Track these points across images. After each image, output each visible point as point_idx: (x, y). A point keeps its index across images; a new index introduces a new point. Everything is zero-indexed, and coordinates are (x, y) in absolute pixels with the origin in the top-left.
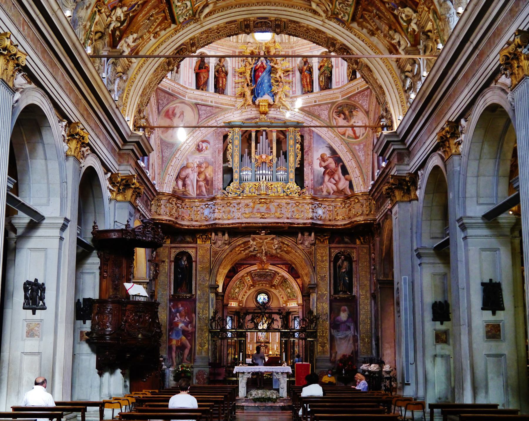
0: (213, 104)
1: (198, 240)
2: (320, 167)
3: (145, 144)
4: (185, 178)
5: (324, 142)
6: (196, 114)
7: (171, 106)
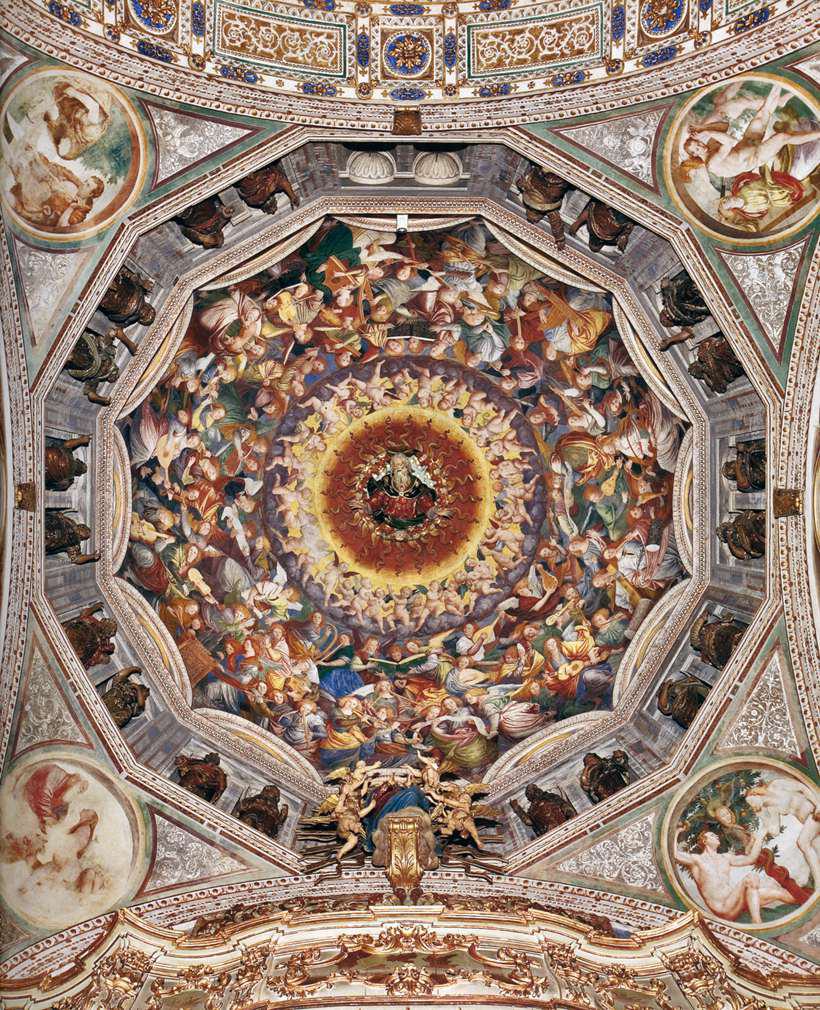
6: (141, 852)
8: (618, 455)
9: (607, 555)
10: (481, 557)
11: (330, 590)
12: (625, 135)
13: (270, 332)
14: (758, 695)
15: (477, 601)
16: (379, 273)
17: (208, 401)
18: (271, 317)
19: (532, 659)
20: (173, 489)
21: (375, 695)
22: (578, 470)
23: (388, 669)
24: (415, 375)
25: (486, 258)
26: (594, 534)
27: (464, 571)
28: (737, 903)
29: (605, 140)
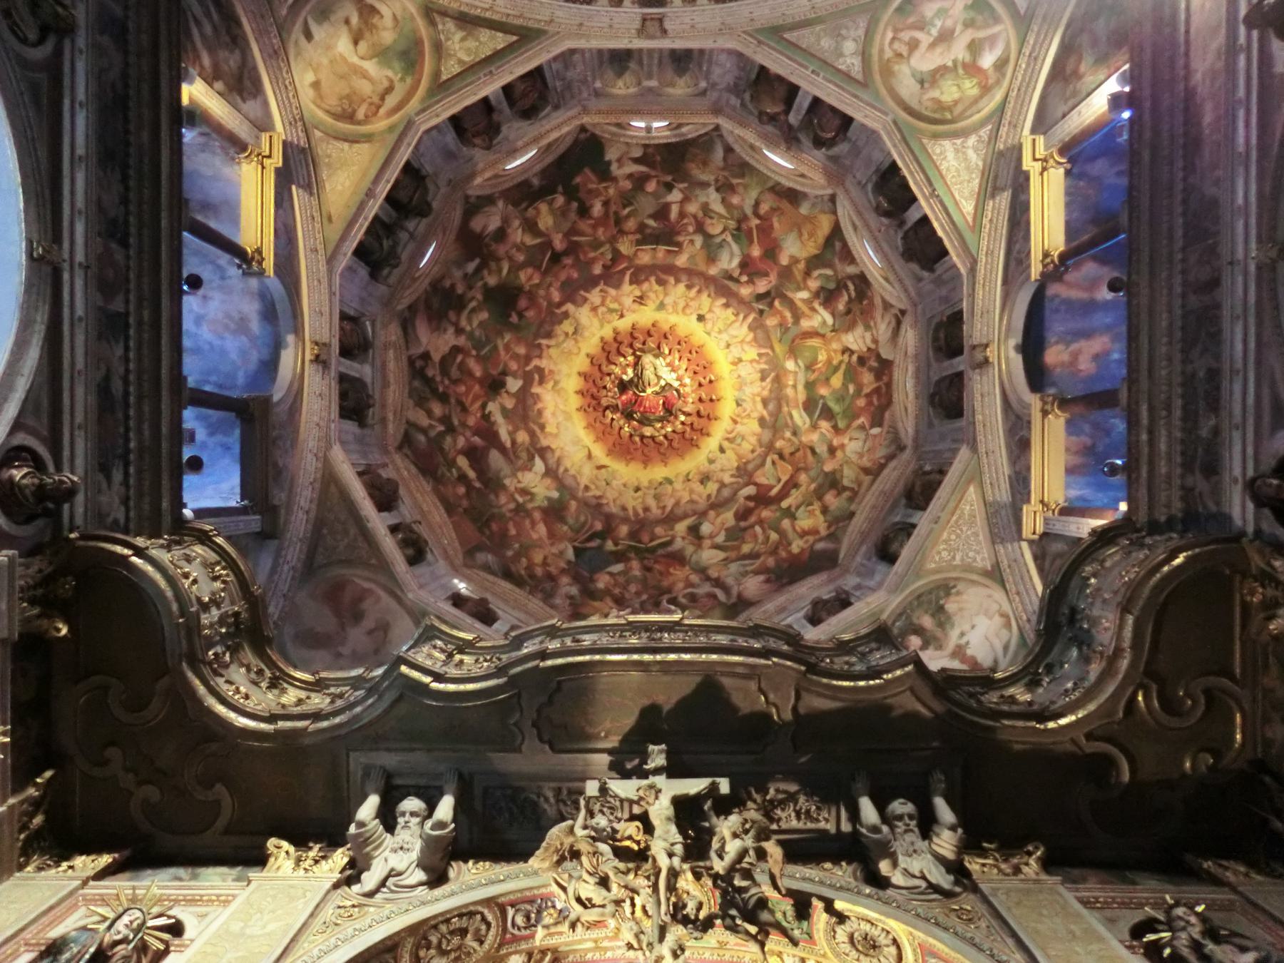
8: (846, 350)
9: (835, 443)
10: (722, 450)
11: (584, 481)
12: (839, 38)
13: (530, 241)
14: (957, 522)
15: (719, 491)
16: (627, 185)
17: (473, 304)
18: (531, 226)
19: (768, 538)
20: (442, 382)
21: (624, 573)
22: (809, 367)
23: (638, 551)
24: (661, 282)
25: (723, 169)
26: (825, 425)
27: (706, 464)
29: (822, 43)
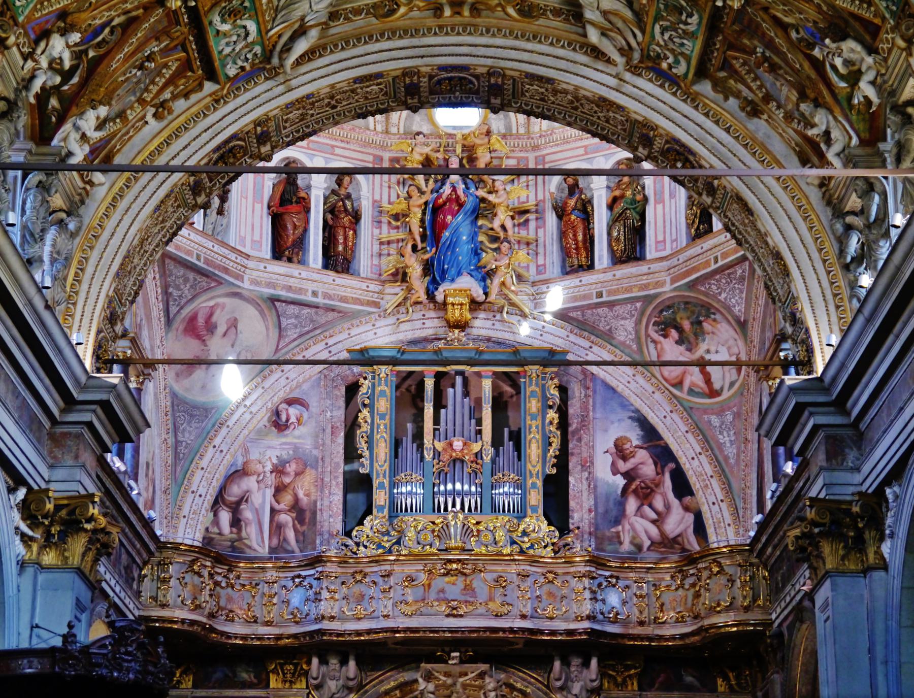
0: (320, 300)
1: (273, 678)
2: (614, 474)
3: (125, 408)
4: (239, 503)
5: (624, 404)
7: (203, 303)
14: (729, 274)
28: (677, 377)
